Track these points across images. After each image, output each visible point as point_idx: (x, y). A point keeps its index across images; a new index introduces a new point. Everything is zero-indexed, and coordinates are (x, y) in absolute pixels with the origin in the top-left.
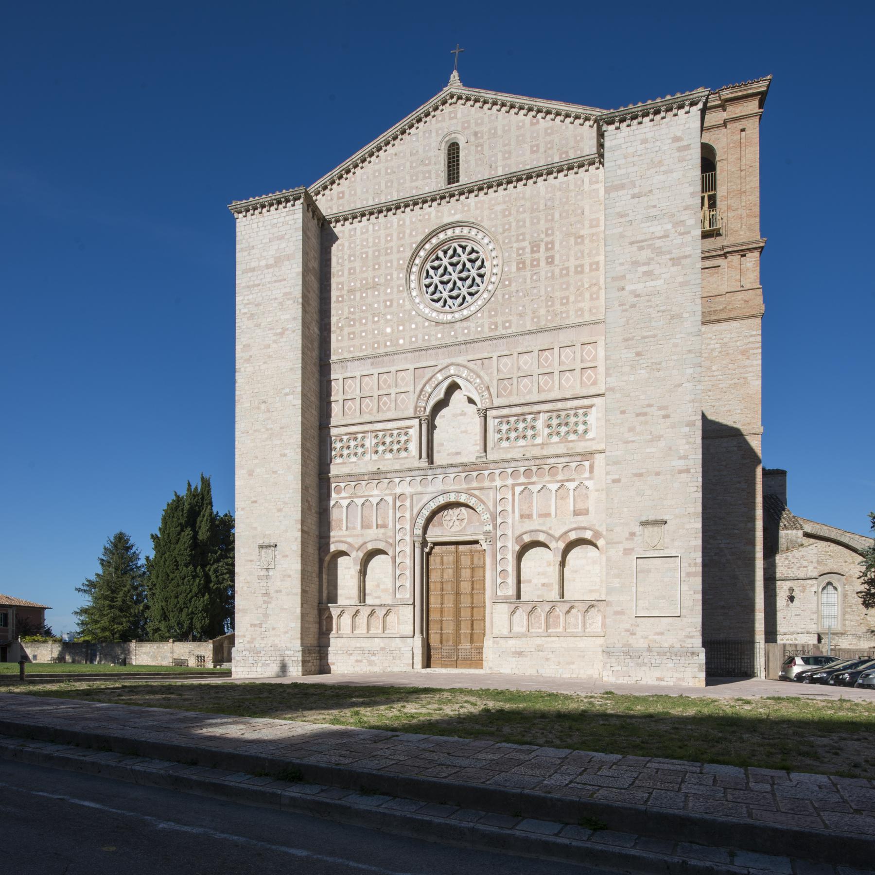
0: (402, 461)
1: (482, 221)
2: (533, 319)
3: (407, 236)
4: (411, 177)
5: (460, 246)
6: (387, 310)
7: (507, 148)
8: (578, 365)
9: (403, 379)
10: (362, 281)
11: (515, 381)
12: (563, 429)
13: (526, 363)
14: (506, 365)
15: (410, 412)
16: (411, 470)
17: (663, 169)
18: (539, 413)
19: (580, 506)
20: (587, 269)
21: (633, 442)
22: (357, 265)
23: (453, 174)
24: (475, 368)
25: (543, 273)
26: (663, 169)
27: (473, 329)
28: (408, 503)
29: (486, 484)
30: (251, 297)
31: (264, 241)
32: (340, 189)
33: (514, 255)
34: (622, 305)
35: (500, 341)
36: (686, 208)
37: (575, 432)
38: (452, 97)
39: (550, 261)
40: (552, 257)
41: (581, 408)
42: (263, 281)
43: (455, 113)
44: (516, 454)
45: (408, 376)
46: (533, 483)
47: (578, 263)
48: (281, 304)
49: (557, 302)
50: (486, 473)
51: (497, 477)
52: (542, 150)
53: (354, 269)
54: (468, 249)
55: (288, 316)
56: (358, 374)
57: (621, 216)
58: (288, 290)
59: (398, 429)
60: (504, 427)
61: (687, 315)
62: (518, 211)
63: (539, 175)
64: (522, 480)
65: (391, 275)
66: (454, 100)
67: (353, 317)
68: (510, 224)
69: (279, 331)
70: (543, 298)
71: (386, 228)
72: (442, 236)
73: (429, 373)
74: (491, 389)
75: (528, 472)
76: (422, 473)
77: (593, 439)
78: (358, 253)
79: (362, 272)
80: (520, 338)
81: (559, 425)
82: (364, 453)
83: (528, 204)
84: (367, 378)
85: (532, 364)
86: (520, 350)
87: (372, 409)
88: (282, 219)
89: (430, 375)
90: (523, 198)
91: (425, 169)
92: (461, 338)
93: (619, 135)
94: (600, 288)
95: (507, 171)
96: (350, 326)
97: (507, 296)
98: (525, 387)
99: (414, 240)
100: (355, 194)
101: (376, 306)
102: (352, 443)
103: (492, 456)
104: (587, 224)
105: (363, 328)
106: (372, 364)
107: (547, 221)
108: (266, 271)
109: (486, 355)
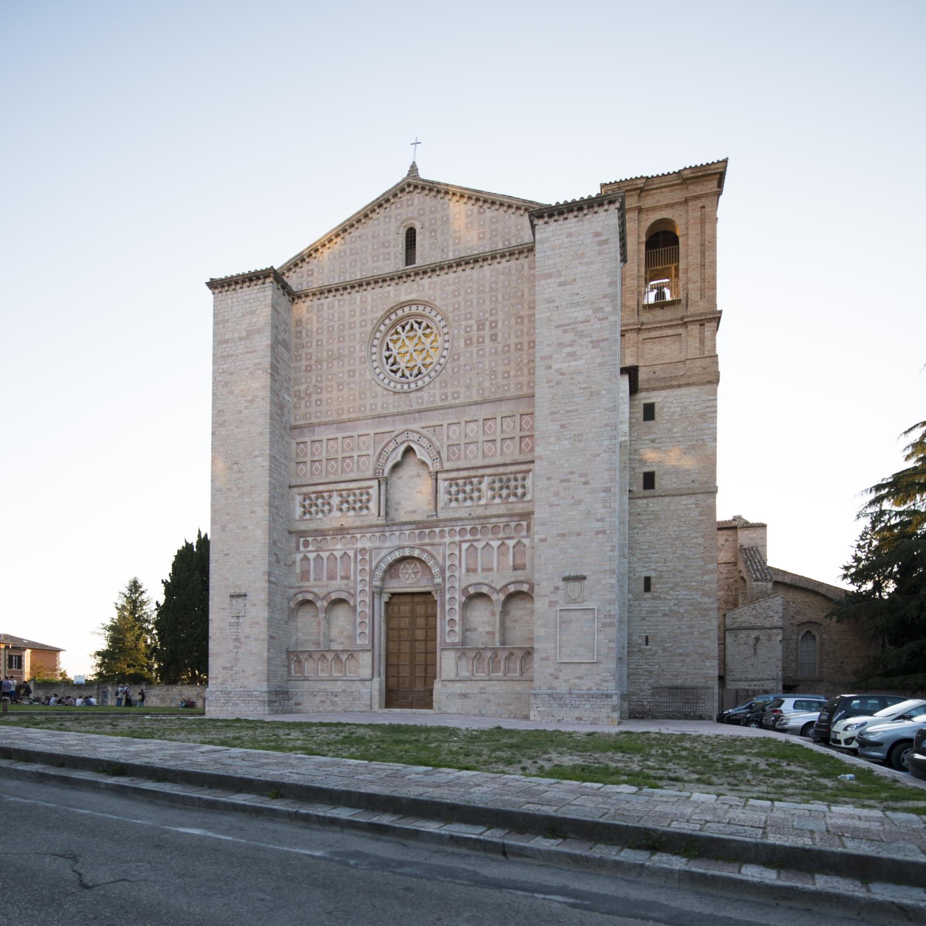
0: (363, 519)
1: (434, 300)
2: (478, 390)
3: (368, 312)
4: (373, 258)
5: (417, 322)
8: (518, 434)
9: (364, 443)
11: (463, 447)
12: (504, 492)
13: (472, 431)
15: (370, 474)
16: (370, 526)
18: (483, 476)
19: (519, 561)
20: (526, 346)
21: (558, 505)
22: (324, 337)
23: (410, 256)
24: (428, 434)
25: (487, 349)
26: (585, 260)
27: (426, 399)
28: (367, 557)
29: (437, 540)
30: (225, 366)
32: (310, 267)
33: (462, 332)
34: (550, 382)
35: (450, 410)
38: (409, 185)
39: (494, 338)
40: (496, 335)
41: (520, 472)
43: (412, 200)
44: (463, 513)
45: (369, 440)
46: (478, 540)
47: (517, 340)
48: (252, 373)
49: (500, 376)
50: (437, 530)
51: (447, 535)
53: (322, 340)
54: (424, 325)
55: (258, 385)
56: (324, 438)
57: (549, 302)
58: (257, 361)
59: (359, 489)
60: (454, 489)
61: (604, 392)
63: (485, 260)
64: (468, 537)
65: (354, 347)
66: (411, 189)
67: (319, 385)
68: (459, 303)
69: (250, 398)
71: (350, 304)
72: (400, 313)
73: (387, 438)
75: (474, 531)
76: (380, 529)
78: (325, 327)
79: (328, 343)
80: (467, 408)
81: (501, 488)
82: (330, 511)
83: (475, 286)
85: (478, 431)
86: (467, 419)
87: (336, 470)
88: (253, 296)
90: (471, 280)
91: (385, 251)
92: (416, 407)
93: (548, 229)
95: (457, 255)
96: (318, 393)
98: (471, 452)
99: (374, 316)
100: (323, 272)
103: (442, 515)
105: (329, 395)
106: (337, 429)
107: (491, 302)
109: (437, 423)
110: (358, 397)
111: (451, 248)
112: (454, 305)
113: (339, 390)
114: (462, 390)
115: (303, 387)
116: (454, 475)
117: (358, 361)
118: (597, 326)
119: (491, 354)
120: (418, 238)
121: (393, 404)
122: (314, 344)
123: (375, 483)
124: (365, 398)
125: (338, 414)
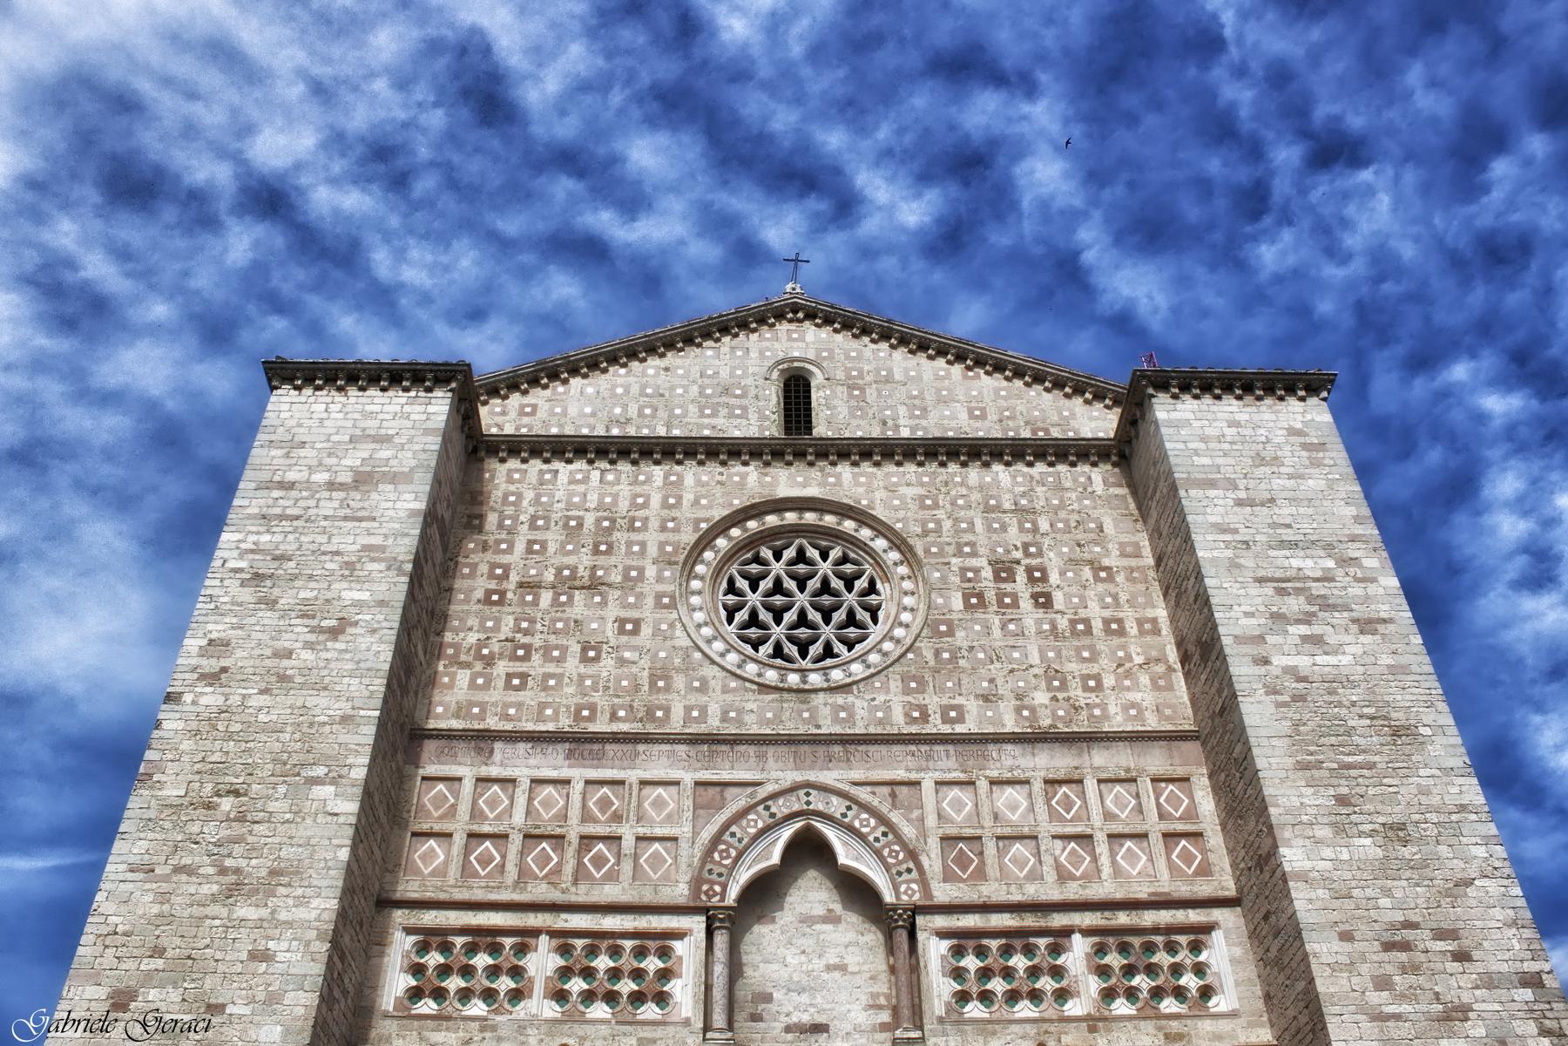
2: (1018, 710)
6: (624, 639)
7: (917, 402)
10: (559, 571)
14: (958, 805)
15: (679, 892)
17: (1282, 470)
18: (1067, 932)
20: (1132, 628)
22: (553, 538)
24: (876, 803)
30: (266, 538)
31: (334, 438)
32: (528, 400)
36: (1353, 539)
37: (1179, 993)
39: (1043, 601)
40: (1048, 596)
42: (311, 512)
47: (1107, 613)
52: (992, 416)
53: (544, 544)
54: (835, 553)
57: (1224, 531)
62: (953, 503)
65: (641, 571)
66: (801, 315)
67: (526, 640)
68: (938, 522)
70: (1035, 671)
73: (737, 801)
74: (924, 860)
77: (1233, 1015)
82: (517, 996)
84: (549, 790)
85: (1031, 808)
86: (994, 774)
87: (558, 870)
89: (742, 803)
91: (733, 401)
94: (1170, 669)
97: (946, 655)
99: (701, 514)
101: (594, 626)
102: (482, 960)
104: (1114, 548)
105: (551, 668)
107: (1022, 529)
108: (326, 494)
109: (900, 774)
110: (646, 682)
111: (902, 422)
112: (924, 524)
113: (585, 659)
114: (972, 706)
115: (472, 638)
116: (970, 921)
117: (650, 601)
118: (1356, 590)
119: (1040, 632)
120: (816, 396)
121: (757, 715)
122: (520, 547)
123: (697, 924)
124: (667, 689)
125: (577, 717)
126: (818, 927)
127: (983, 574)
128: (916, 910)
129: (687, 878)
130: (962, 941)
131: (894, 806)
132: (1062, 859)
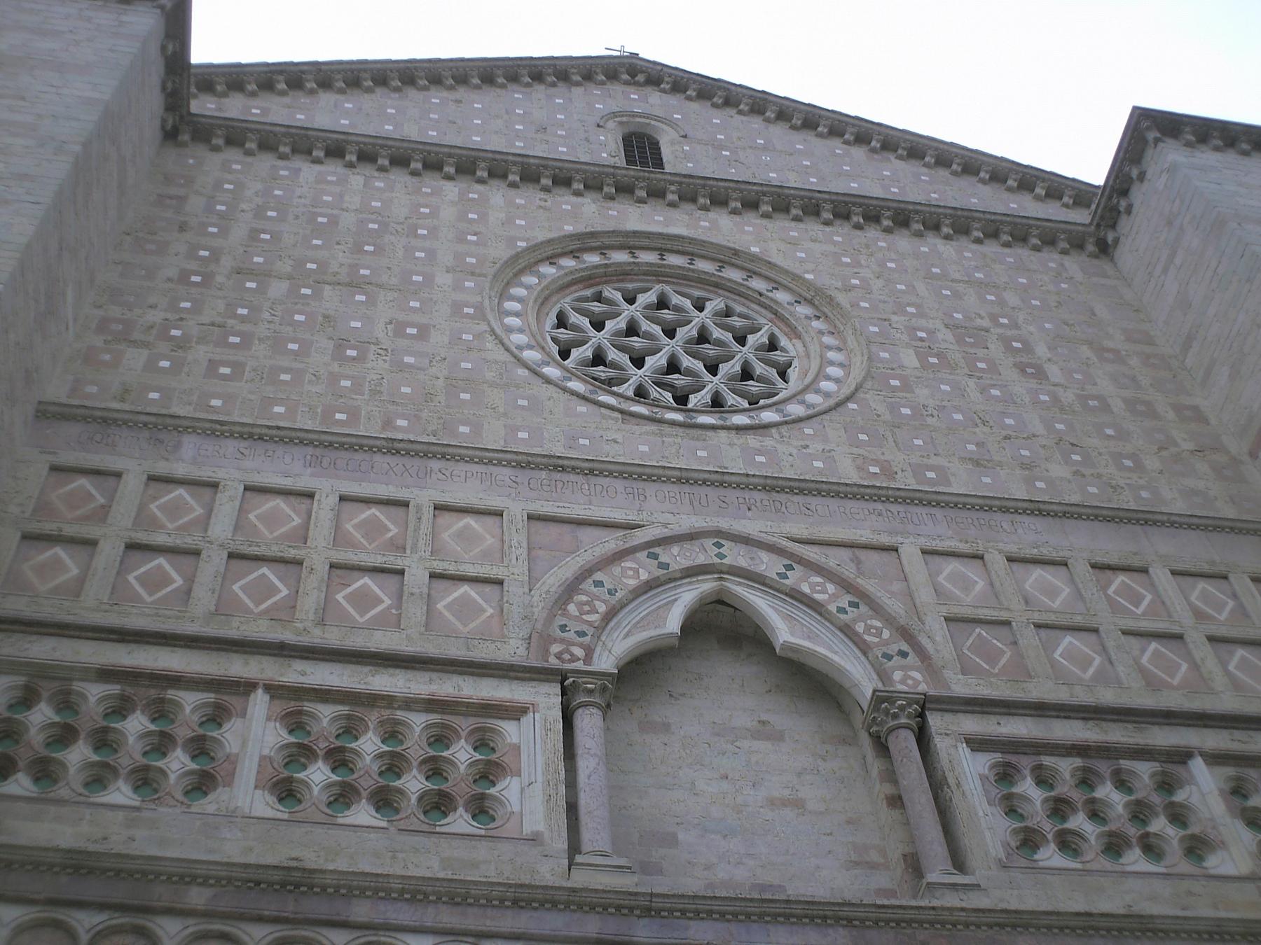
15: (513, 650)
18: (1182, 756)
86: (1013, 549)
123: (547, 699)
126: (745, 744)
127: (940, 336)
128: (925, 705)
129: (524, 633)
130: (1009, 759)
131: (860, 573)
132: (1145, 660)
